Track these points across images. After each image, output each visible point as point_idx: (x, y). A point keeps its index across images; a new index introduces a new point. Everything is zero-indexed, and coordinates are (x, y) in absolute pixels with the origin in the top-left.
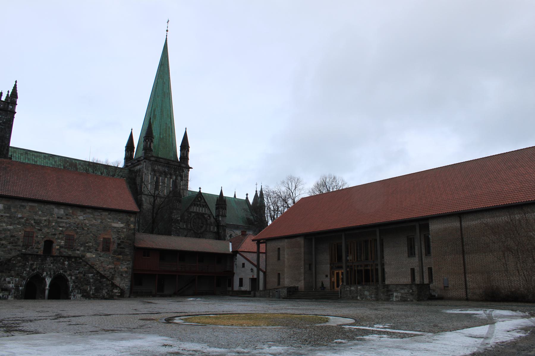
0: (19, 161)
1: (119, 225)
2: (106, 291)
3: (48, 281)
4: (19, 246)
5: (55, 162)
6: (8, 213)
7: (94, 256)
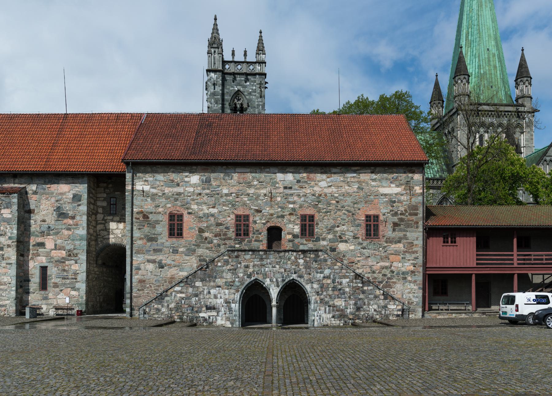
1: (394, 190)
2: (375, 307)
3: (274, 293)
4: (230, 239)
6: (208, 189)
7: (352, 247)
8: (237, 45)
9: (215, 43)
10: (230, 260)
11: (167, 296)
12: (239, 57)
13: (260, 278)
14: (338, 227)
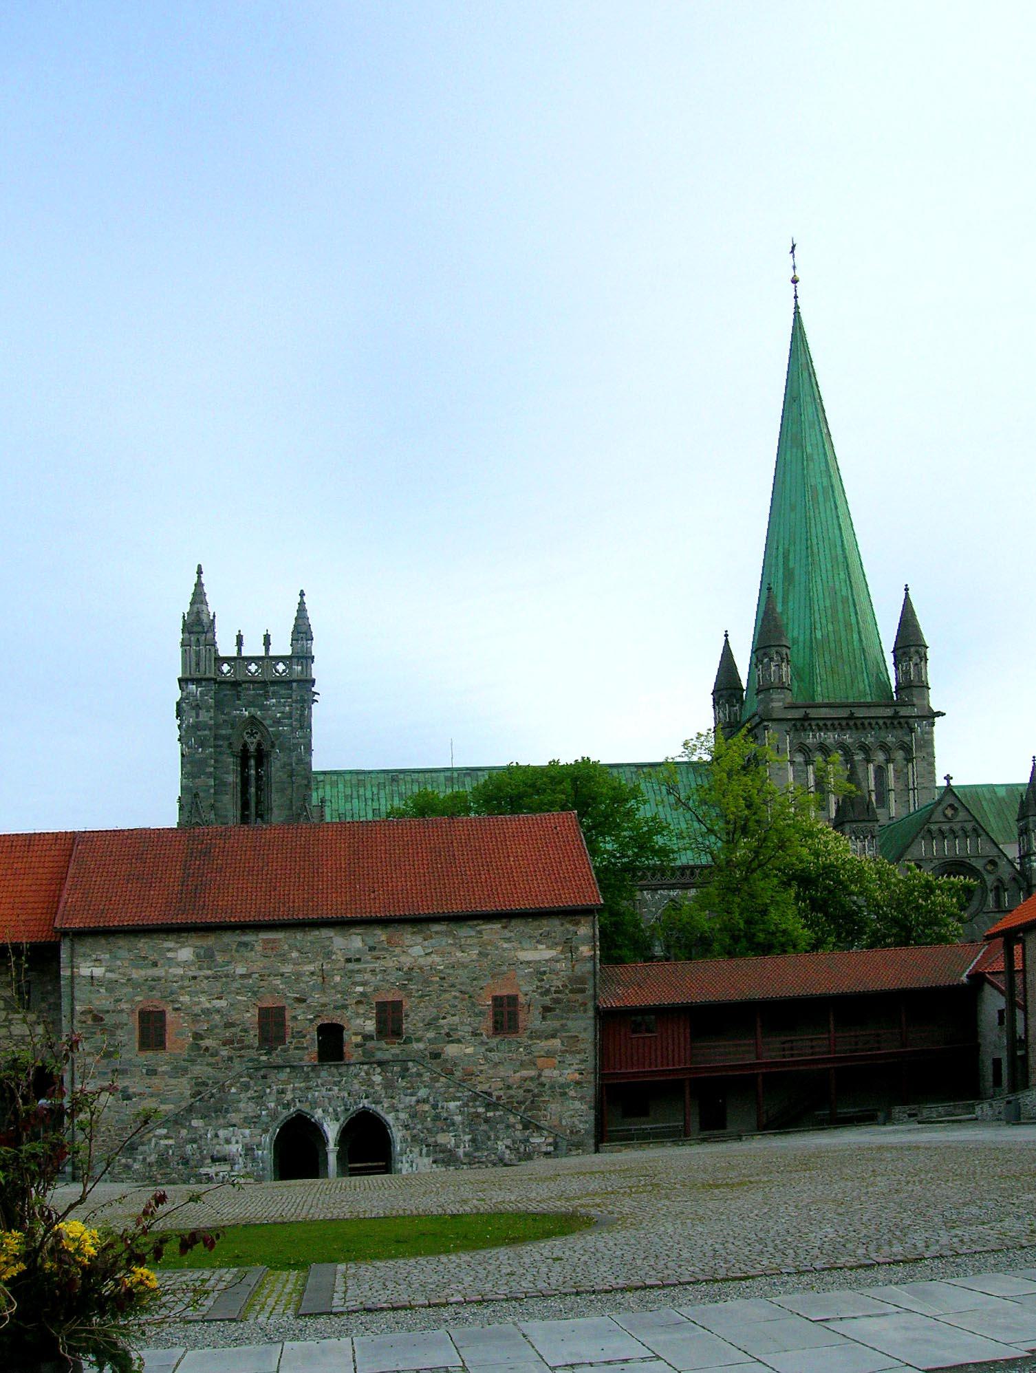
4: (249, 1047)
7: (470, 1050)
9: (198, 627)
10: (252, 1083)
13: (306, 1108)
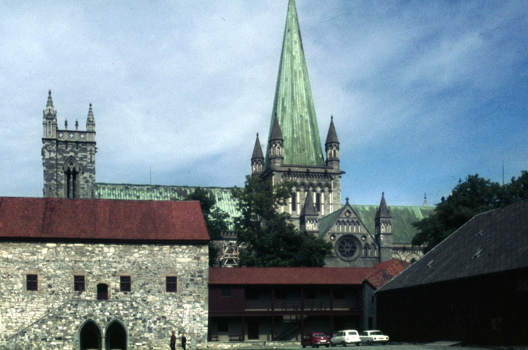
0: (120, 198)
5: (161, 193)
8: (70, 116)
11: (28, 330)
12: (71, 127)
14: (147, 284)
